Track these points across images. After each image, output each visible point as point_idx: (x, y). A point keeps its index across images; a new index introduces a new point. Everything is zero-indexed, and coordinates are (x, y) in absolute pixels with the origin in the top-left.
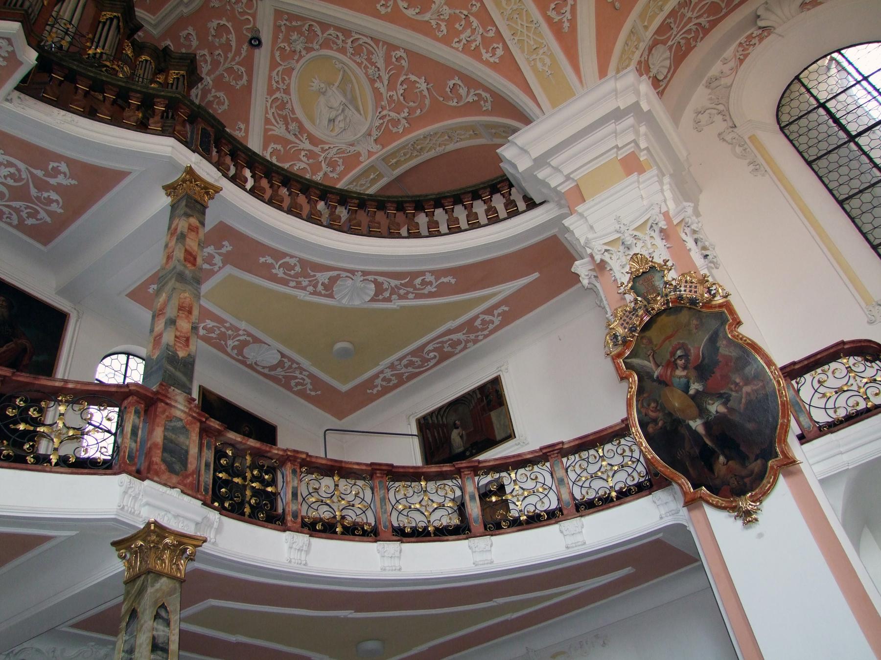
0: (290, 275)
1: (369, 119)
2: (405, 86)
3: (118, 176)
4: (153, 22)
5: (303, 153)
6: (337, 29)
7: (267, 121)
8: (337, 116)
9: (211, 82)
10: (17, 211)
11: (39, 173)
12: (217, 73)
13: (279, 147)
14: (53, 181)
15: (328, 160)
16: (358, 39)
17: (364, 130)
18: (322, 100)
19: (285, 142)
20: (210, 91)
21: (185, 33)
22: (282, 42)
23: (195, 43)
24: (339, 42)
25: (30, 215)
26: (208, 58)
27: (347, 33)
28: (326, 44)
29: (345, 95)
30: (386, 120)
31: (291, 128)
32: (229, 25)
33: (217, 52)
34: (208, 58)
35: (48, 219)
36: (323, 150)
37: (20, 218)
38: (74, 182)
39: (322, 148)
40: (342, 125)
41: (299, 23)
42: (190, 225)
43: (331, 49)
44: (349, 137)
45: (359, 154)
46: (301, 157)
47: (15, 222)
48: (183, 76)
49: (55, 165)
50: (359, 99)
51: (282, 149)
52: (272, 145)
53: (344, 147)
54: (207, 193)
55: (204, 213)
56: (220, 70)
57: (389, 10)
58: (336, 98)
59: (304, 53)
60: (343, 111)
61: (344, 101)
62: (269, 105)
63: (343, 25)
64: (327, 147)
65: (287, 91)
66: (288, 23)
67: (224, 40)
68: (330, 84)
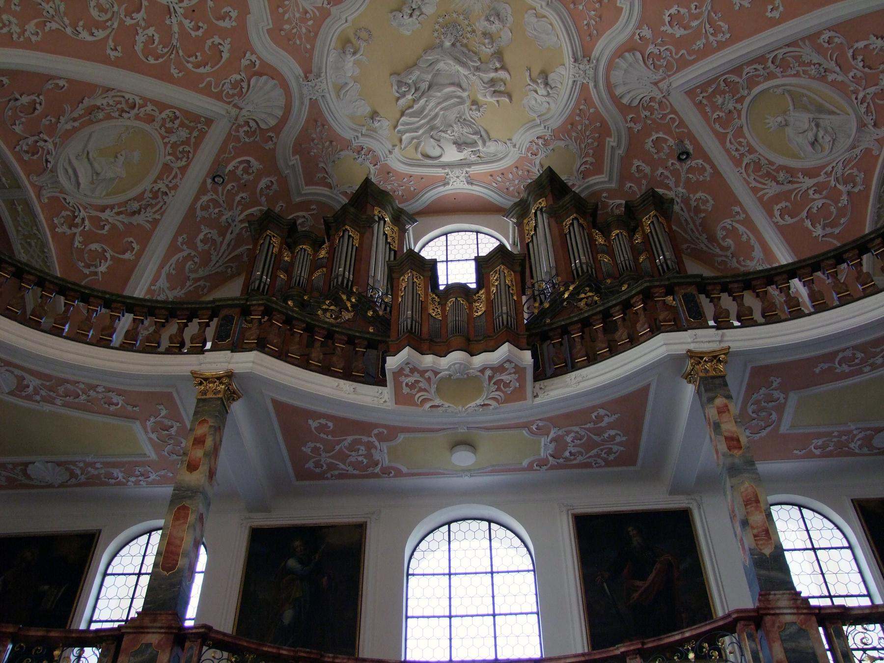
0: (858, 364)
1: (850, 111)
2: (860, 58)
3: (644, 392)
4: (607, 179)
5: (811, 192)
6: (749, 63)
7: (755, 190)
8: (816, 136)
9: (684, 191)
11: (587, 426)
12: (683, 180)
13: (783, 204)
14: (603, 424)
15: (840, 179)
16: (776, 56)
17: (854, 125)
18: (789, 131)
19: (785, 195)
20: (688, 199)
21: (634, 168)
22: (713, 113)
23: (647, 170)
24: (762, 72)
25: (608, 454)
26: (666, 173)
27: (760, 59)
28: (752, 83)
29: (806, 109)
30: (868, 100)
31: (780, 179)
32: (661, 135)
33: (670, 164)
34: (666, 173)
35: (622, 448)
36: (828, 174)
38: (616, 416)
39: (826, 173)
40: (828, 138)
41: (714, 86)
42: (718, 408)
43: (758, 83)
44: (844, 143)
45: (868, 151)
46: (811, 196)
47: (603, 463)
48: (655, 216)
49: (595, 414)
50: (827, 104)
51: (787, 204)
52: (776, 207)
53: (847, 155)
54: (719, 361)
55: (726, 385)
56: (683, 175)
57: (781, 9)
58: (803, 119)
59: (738, 106)
60: (817, 125)
61: (811, 116)
62: (745, 175)
63: (753, 56)
64: (829, 169)
65: (751, 150)
66: (705, 94)
67: (666, 150)
68: (785, 112)
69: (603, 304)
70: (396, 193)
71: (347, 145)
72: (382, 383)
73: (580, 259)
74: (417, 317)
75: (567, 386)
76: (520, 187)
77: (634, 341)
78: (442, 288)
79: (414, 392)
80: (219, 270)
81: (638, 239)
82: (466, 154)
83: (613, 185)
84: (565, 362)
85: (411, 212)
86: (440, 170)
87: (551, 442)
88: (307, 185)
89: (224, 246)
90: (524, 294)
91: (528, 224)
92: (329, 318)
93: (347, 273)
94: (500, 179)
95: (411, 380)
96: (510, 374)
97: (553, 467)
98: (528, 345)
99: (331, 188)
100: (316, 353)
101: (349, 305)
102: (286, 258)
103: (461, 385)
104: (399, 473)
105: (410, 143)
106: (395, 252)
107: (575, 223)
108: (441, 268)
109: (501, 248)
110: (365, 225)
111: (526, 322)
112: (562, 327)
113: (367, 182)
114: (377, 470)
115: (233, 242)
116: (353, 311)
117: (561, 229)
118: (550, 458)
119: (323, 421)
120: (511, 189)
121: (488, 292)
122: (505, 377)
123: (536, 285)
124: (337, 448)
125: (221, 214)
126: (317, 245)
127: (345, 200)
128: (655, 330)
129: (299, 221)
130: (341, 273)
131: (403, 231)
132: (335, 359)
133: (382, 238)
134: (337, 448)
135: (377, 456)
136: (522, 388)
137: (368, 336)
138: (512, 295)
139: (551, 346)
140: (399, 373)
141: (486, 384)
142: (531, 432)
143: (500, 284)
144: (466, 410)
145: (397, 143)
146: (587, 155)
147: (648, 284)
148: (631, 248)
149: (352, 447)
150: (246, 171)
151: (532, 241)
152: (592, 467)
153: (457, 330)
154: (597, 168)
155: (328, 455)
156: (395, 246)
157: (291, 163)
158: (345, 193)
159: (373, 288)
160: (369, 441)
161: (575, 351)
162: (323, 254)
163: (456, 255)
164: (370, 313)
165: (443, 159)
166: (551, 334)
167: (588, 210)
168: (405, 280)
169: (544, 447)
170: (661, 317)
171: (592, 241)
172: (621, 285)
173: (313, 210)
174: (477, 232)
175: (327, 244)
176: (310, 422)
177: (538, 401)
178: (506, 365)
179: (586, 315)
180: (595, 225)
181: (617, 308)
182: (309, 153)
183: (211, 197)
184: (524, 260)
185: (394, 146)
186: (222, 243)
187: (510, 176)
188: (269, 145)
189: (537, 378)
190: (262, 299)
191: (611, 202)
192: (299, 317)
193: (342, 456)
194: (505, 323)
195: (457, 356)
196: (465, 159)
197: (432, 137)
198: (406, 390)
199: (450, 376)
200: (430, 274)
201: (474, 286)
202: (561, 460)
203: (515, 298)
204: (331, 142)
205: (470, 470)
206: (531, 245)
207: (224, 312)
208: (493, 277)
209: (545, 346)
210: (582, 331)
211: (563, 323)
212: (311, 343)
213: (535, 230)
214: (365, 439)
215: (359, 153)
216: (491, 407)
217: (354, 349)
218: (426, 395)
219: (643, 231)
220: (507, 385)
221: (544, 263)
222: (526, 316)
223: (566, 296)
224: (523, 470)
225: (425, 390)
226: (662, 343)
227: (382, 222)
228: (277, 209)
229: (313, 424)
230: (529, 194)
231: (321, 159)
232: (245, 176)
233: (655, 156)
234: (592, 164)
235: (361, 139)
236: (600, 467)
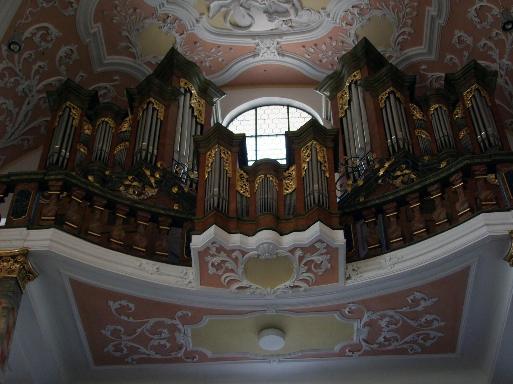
4: (426, 51)
9: (509, 63)
10: (414, 342)
11: (405, 309)
12: (508, 51)
14: (420, 308)
21: (455, 39)
23: (469, 40)
26: (490, 44)
33: (493, 34)
34: (490, 44)
35: (440, 334)
37: (419, 345)
38: (434, 300)
47: (420, 350)
49: (412, 297)
67: (490, 19)
69: (420, 182)
70: (204, 64)
71: (152, 12)
72: (188, 263)
73: (397, 135)
74: (224, 194)
75: (381, 268)
76: (333, 58)
77: (453, 221)
78: (250, 164)
79: (220, 272)
80: (15, 143)
81: (458, 114)
82: (277, 23)
83: (432, 57)
84: (380, 242)
85: (218, 84)
86: (249, 40)
87: (364, 326)
88: (109, 54)
89: (21, 118)
90: (336, 171)
91: (342, 97)
92: (131, 195)
93: (151, 147)
94: (312, 51)
95: (217, 260)
96: (322, 254)
97: (366, 353)
98: (341, 224)
99: (134, 58)
100: (117, 231)
101: (153, 181)
102: (87, 132)
103: (270, 265)
104: (204, 358)
105: (218, 11)
106: (202, 126)
107: (392, 97)
108: (250, 144)
109: (313, 122)
110: (170, 98)
111: (338, 200)
112: (376, 205)
113: (173, 52)
114: (181, 354)
115: (30, 114)
116: (156, 187)
117: (376, 103)
118: (364, 344)
119: (124, 303)
120: (325, 60)
121: (299, 169)
122: (316, 258)
123: (350, 162)
124: (139, 331)
125: (17, 83)
126: (120, 118)
127: (149, 71)
128: (476, 210)
129: (101, 93)
130: (145, 147)
131: (210, 104)
132: (137, 237)
133: (188, 111)
134: (139, 331)
135: (180, 339)
136: (334, 269)
137: (173, 214)
138: (325, 172)
139: (365, 225)
140: (204, 252)
141: (296, 265)
142: (343, 315)
143: (311, 160)
144: (275, 292)
145: (205, 11)
146: (405, 25)
147: (468, 161)
148: (451, 122)
149: (155, 330)
150: (44, 38)
151: (346, 115)
152: (408, 353)
153: (266, 208)
154: (416, 39)
155: (129, 338)
156: (202, 120)
157: (92, 31)
158: (149, 64)
159: (178, 164)
160: (172, 324)
161: (391, 230)
162: (125, 127)
163: (266, 130)
164: (175, 190)
165: (255, 29)
166: (365, 213)
167: (405, 84)
168: (212, 155)
169: (357, 331)
170: (482, 196)
171: (409, 115)
172: (440, 163)
173: (116, 80)
174: (288, 106)
175: (130, 117)
176: (111, 303)
177: (350, 283)
178: (318, 245)
179: (402, 193)
180: (412, 99)
181: (436, 186)
182: (112, 20)
183: (6, 65)
184: (337, 136)
185: (202, 14)
186: (18, 114)
187: (324, 47)
188: (69, 12)
189: (349, 259)
190: (61, 174)
191: (430, 74)
192: (100, 193)
193: (144, 340)
194: (317, 201)
195: (265, 236)
196: (276, 29)
197: (241, 5)
198: (212, 271)
199: (259, 256)
200: (237, 149)
201: (284, 162)
202: (375, 346)
203: (327, 175)
204: (135, 9)
205: (278, 355)
206: (344, 119)
207: (20, 187)
208: (305, 154)
209: (358, 226)
210: (398, 210)
211: (377, 202)
212: (112, 220)
213: (349, 104)
214: (169, 321)
215: (164, 21)
216: (301, 289)
217: (158, 227)
218: (233, 276)
219: (464, 105)
220: (318, 266)
221: (358, 139)
222: (339, 194)
223: (381, 173)
224: (335, 355)
225: (232, 271)
226: (483, 223)
227: (188, 95)
228: (77, 80)
229: (114, 305)
230: (343, 67)
231: (124, 27)
232: (43, 44)
233: (479, 26)
234: (410, 34)
235: (167, 7)
236: (417, 353)
